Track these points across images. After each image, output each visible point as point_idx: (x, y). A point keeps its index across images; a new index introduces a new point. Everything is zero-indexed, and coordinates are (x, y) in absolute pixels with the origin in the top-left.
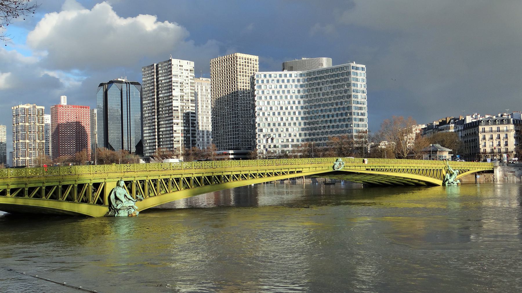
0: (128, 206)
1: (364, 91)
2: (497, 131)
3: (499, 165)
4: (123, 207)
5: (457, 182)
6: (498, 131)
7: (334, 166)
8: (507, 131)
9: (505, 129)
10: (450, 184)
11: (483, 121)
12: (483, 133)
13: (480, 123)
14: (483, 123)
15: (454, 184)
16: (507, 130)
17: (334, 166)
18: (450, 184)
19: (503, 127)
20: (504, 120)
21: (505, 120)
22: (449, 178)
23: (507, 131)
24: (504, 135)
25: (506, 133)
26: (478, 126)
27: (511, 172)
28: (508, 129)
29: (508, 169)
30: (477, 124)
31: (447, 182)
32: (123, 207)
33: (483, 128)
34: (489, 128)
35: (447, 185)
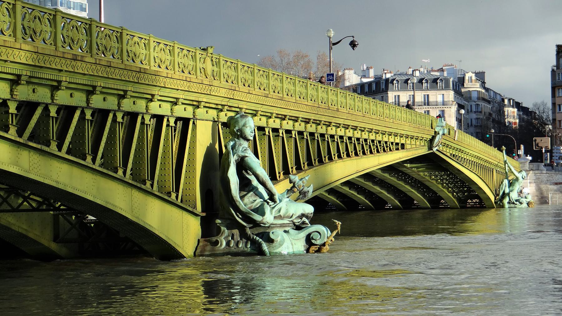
0: (299, 213)
1: (84, 6)
2: (423, 104)
3: (529, 168)
4: (280, 217)
5: (528, 200)
6: (425, 105)
7: (434, 138)
8: (444, 103)
9: (440, 99)
10: (512, 205)
11: (397, 81)
12: (425, 107)
13: (390, 85)
14: (397, 85)
15: (521, 203)
16: (443, 101)
17: (434, 138)
18: (514, 203)
19: (436, 96)
20: (438, 81)
21: (441, 79)
22: (507, 191)
23: (444, 103)
24: (438, 111)
25: (443, 109)
26: (386, 90)
27: (556, 184)
28: (445, 100)
29: (550, 176)
30: (383, 86)
31: (506, 200)
32: (280, 217)
33: (395, 96)
34: (423, 96)
35: (507, 206)
